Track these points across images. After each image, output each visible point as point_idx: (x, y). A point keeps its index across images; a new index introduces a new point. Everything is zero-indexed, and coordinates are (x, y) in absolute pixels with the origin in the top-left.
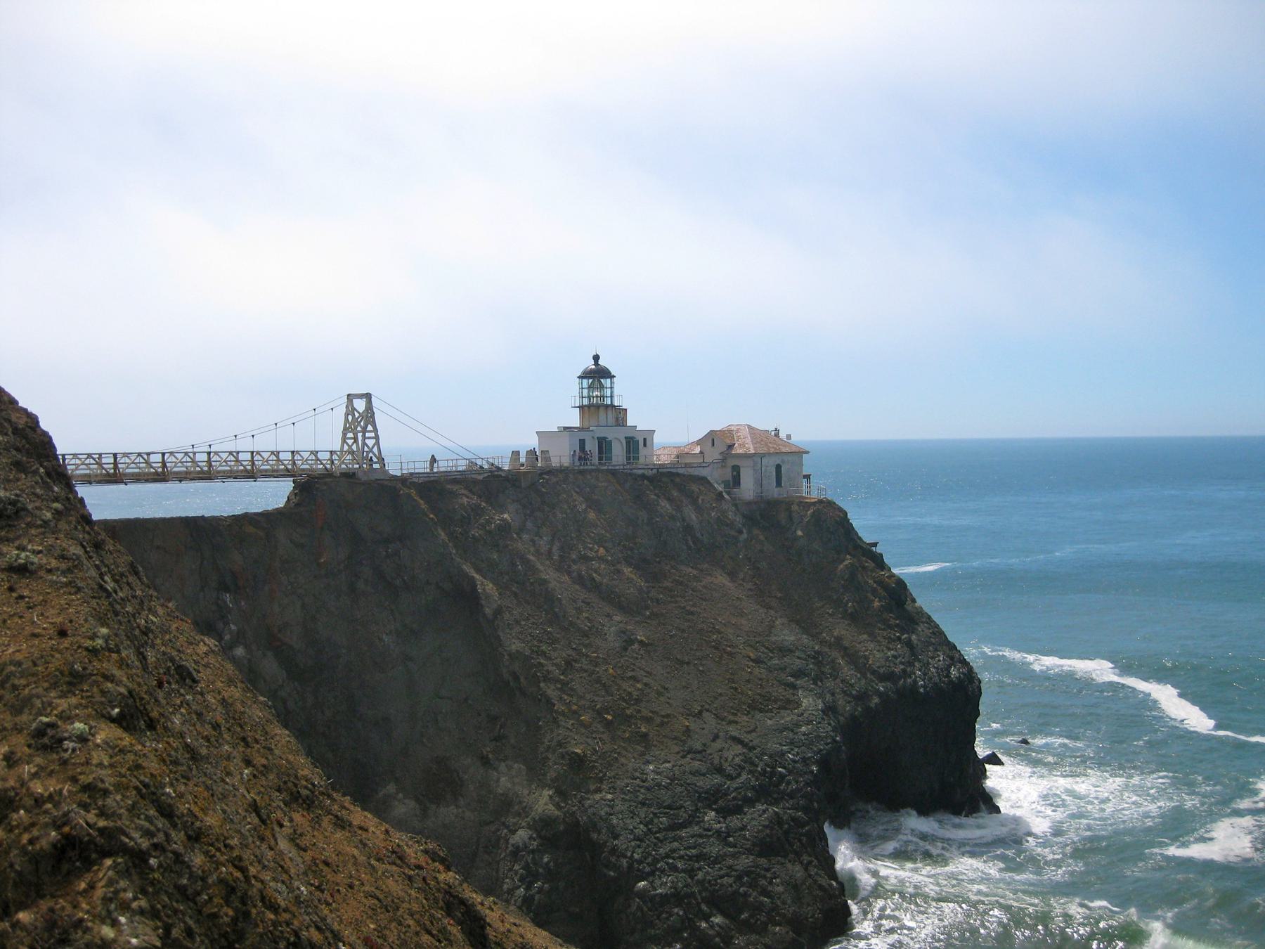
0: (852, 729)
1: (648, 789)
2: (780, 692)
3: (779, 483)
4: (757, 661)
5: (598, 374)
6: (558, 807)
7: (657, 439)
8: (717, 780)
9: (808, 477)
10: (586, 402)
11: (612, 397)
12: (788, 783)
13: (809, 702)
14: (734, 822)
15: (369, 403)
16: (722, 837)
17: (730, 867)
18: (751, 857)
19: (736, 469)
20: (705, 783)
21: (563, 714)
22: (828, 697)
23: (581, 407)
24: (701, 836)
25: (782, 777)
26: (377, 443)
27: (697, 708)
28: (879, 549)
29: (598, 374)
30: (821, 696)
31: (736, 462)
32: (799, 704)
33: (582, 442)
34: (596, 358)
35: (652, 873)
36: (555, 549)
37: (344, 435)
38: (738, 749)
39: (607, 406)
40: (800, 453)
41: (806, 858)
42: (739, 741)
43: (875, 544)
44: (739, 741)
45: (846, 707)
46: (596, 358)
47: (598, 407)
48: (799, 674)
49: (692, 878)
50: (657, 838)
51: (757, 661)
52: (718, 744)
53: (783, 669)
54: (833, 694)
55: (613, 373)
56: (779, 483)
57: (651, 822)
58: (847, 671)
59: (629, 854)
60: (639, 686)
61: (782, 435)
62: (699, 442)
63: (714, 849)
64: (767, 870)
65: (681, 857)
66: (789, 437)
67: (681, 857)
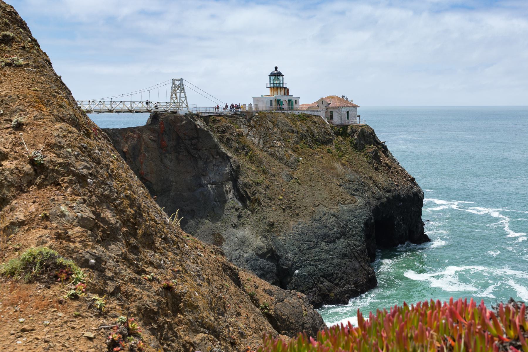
0: (376, 211)
1: (299, 234)
2: (349, 197)
3: (348, 118)
4: (340, 185)
5: (277, 75)
6: (263, 242)
7: (301, 102)
8: (326, 230)
9: (359, 116)
10: (272, 85)
11: (282, 84)
12: (353, 231)
13: (360, 201)
14: (332, 246)
15: (182, 83)
16: (328, 252)
17: (331, 263)
18: (339, 260)
19: (332, 113)
20: (321, 232)
21: (265, 206)
22: (367, 199)
23: (270, 88)
24: (319, 252)
25: (350, 229)
26: (186, 99)
27: (317, 203)
28: (385, 144)
29: (277, 75)
30: (364, 199)
31: (331, 110)
32: (356, 202)
33: (271, 101)
34: (276, 68)
35: (301, 267)
36: (260, 142)
37: (172, 95)
38: (334, 219)
39: (281, 88)
40: (356, 107)
41: (360, 259)
42: (334, 216)
43: (384, 142)
44: (334, 216)
45: (374, 202)
46: (276, 68)
47: (277, 88)
48: (356, 190)
49: (316, 268)
50: (303, 253)
51: (340, 185)
52: (325, 218)
53: (350, 189)
54: (369, 198)
55: (283, 74)
56: (348, 118)
57: (300, 247)
58: (375, 189)
59: (292, 259)
60: (295, 195)
61: (349, 100)
62: (317, 102)
63: (324, 256)
64: (345, 264)
65: (312, 260)
66: (352, 101)
67: (312, 260)
